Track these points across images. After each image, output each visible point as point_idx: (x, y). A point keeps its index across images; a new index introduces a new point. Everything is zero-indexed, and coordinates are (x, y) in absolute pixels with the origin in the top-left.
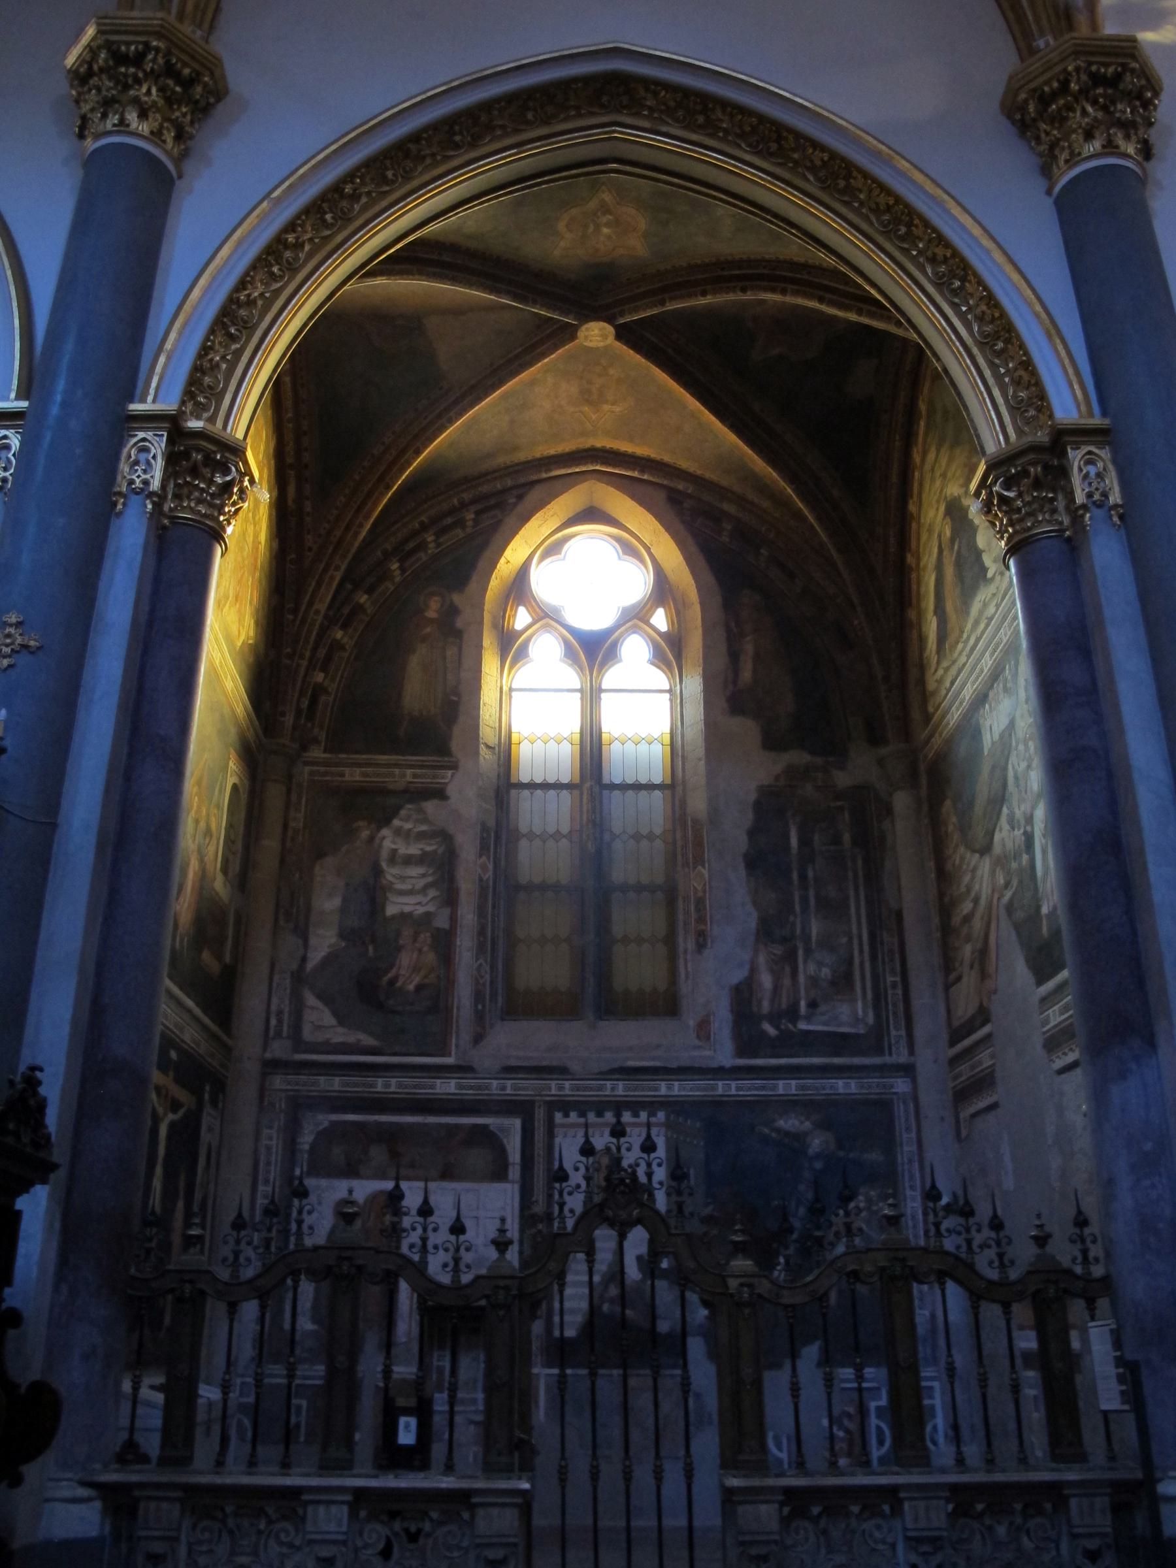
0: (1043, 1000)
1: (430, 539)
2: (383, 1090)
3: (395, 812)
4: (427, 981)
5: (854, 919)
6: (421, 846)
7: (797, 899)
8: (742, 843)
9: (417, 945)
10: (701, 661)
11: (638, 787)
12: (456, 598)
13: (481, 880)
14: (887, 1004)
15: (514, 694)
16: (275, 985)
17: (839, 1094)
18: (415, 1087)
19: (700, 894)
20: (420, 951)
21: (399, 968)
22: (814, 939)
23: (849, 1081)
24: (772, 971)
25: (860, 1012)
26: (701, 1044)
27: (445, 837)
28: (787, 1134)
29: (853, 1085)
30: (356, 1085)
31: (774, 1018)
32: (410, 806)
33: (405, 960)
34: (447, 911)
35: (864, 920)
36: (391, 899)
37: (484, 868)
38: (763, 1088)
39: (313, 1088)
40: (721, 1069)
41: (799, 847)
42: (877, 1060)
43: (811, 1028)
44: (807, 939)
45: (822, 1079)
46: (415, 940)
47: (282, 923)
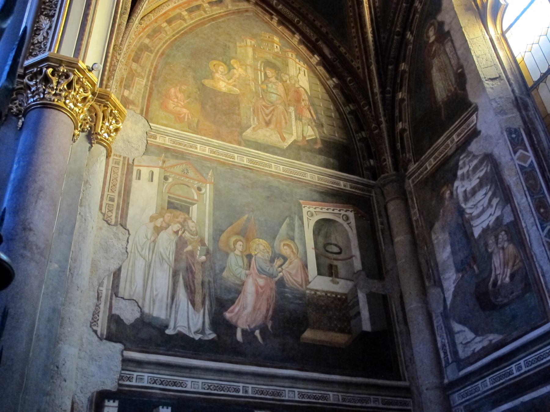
1: (417, 5)
2: (518, 373)
3: (456, 167)
4: (515, 268)
6: (477, 176)
9: (500, 246)
12: (440, 18)
13: (522, 168)
15: (507, 35)
16: (436, 328)
18: (538, 359)
20: (503, 248)
21: (495, 270)
27: (489, 158)
30: (500, 378)
32: (461, 157)
33: (497, 261)
34: (508, 209)
36: (474, 225)
37: (523, 158)
39: (476, 394)
46: (497, 243)
47: (427, 284)
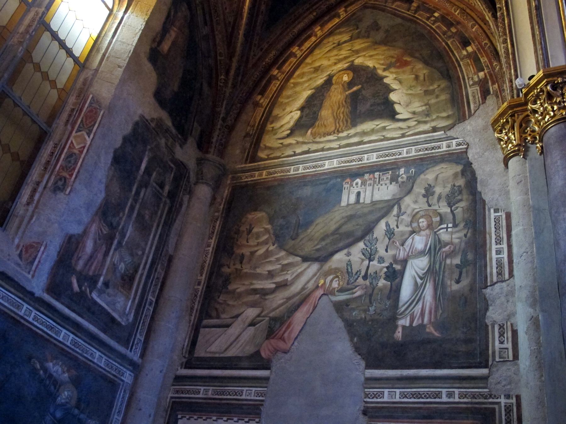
0: (368, 379)
5: (149, 243)
7: (129, 204)
8: (118, 143)
10: (149, 13)
11: (62, 44)
14: (142, 313)
17: (93, 363)
19: (76, 152)
22: (126, 239)
23: (103, 356)
24: (95, 242)
25: (128, 309)
26: (21, 263)
28: (51, 376)
29: (103, 360)
31: (82, 278)
35: (154, 248)
38: (51, 328)
40: (32, 294)
41: (144, 173)
42: (121, 349)
43: (98, 300)
44: (123, 235)
45: (89, 344)
